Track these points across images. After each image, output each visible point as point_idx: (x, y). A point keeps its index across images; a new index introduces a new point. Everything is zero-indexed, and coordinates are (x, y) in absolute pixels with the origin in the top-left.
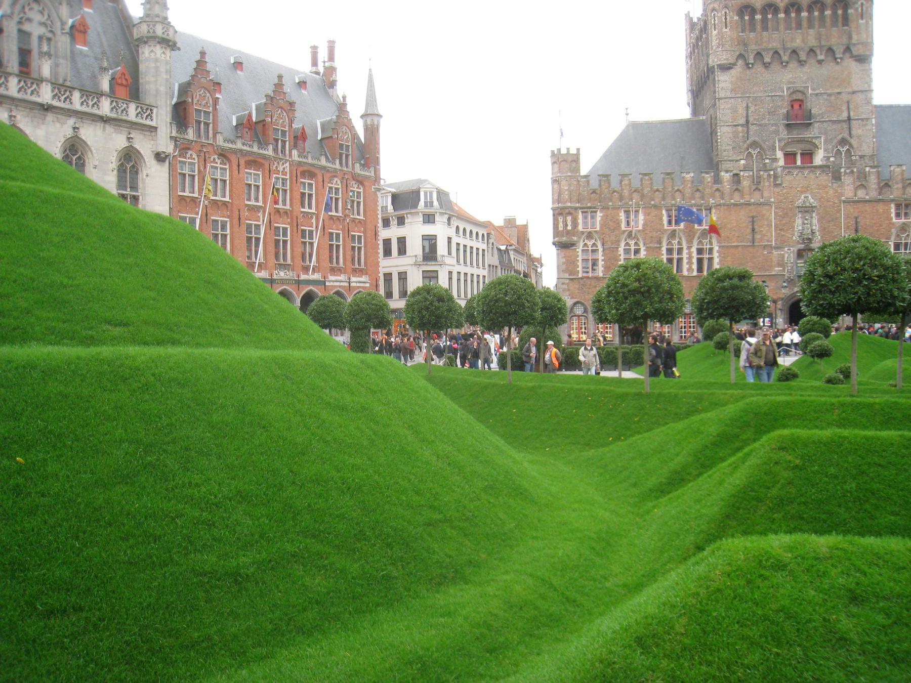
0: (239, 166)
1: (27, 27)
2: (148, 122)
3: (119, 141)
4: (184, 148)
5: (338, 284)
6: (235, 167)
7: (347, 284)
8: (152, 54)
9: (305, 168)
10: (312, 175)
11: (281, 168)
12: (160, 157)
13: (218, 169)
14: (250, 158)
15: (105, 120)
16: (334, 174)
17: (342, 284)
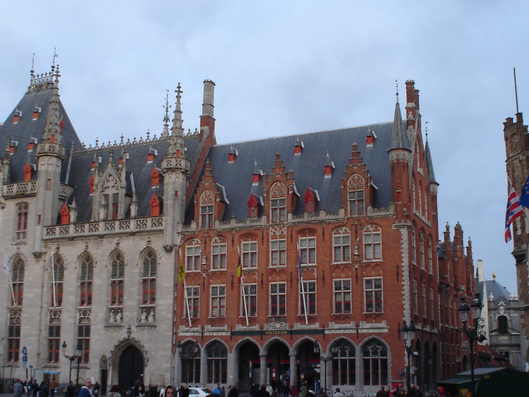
0: (233, 241)
1: (107, 192)
2: (160, 228)
3: (143, 244)
4: (188, 239)
5: (342, 332)
6: (230, 242)
7: (355, 332)
8: (170, 179)
9: (303, 226)
10: (312, 231)
11: (278, 233)
12: (168, 250)
13: (218, 248)
14: (244, 232)
15: (133, 234)
16: (339, 225)
17: (347, 332)
